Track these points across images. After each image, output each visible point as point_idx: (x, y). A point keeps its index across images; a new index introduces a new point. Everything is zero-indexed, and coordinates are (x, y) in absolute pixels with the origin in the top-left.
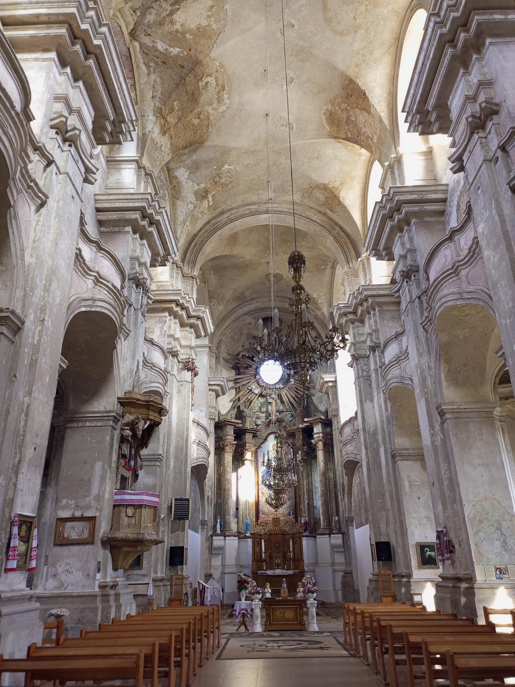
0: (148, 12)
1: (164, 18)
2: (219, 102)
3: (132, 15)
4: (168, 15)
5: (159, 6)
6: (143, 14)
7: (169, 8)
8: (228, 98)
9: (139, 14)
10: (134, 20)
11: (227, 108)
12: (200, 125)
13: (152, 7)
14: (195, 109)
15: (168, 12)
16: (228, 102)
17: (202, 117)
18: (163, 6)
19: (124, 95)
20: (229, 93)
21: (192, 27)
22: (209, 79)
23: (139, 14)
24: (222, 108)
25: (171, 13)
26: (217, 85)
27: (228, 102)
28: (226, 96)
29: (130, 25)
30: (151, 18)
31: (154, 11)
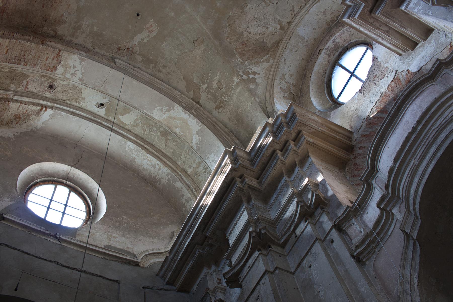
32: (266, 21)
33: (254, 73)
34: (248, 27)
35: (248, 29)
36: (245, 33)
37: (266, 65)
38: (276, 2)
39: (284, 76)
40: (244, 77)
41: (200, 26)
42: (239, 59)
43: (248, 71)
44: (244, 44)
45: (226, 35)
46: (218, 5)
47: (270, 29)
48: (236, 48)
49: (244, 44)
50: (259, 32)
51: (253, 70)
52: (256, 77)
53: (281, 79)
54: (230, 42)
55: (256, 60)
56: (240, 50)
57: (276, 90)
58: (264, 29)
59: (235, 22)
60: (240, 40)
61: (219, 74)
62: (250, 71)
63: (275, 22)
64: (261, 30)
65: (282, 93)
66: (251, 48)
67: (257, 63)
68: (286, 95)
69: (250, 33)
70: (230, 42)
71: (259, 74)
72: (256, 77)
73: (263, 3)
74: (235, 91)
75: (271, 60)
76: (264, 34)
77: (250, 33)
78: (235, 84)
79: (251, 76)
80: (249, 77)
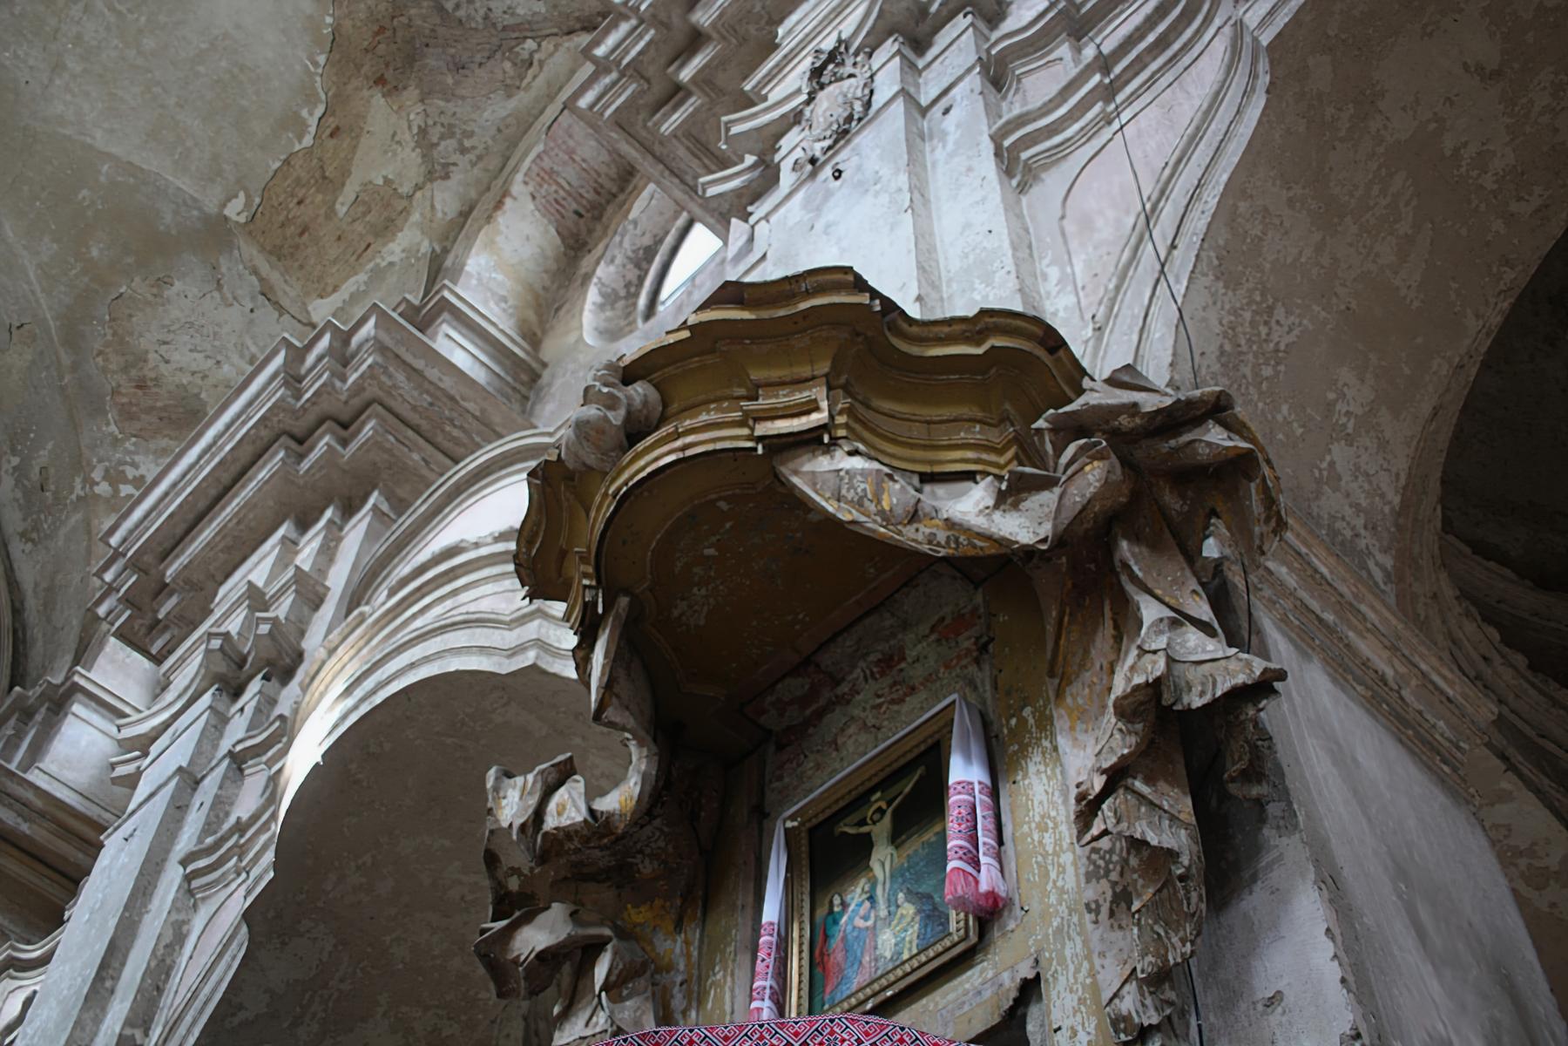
3: (541, 63)
10: (557, 47)
13: (486, 18)
19: (228, 427)
23: (530, 44)
32: (217, 343)
34: (165, 343)
35: (164, 347)
36: (152, 356)
38: (250, 306)
40: (103, 488)
41: (33, 292)
42: (113, 428)
43: (123, 472)
44: (141, 385)
45: (97, 346)
46: (95, 253)
47: (226, 367)
48: (115, 392)
49: (141, 385)
50: (194, 367)
54: (104, 370)
55: (164, 442)
56: (125, 400)
58: (210, 363)
59: (131, 316)
60: (133, 373)
61: (50, 446)
62: (131, 473)
63: (242, 356)
64: (200, 362)
66: (159, 404)
69: (167, 362)
70: (104, 370)
73: (216, 294)
74: (67, 517)
76: (205, 377)
77: (167, 362)
78: (74, 497)
80: (116, 491)
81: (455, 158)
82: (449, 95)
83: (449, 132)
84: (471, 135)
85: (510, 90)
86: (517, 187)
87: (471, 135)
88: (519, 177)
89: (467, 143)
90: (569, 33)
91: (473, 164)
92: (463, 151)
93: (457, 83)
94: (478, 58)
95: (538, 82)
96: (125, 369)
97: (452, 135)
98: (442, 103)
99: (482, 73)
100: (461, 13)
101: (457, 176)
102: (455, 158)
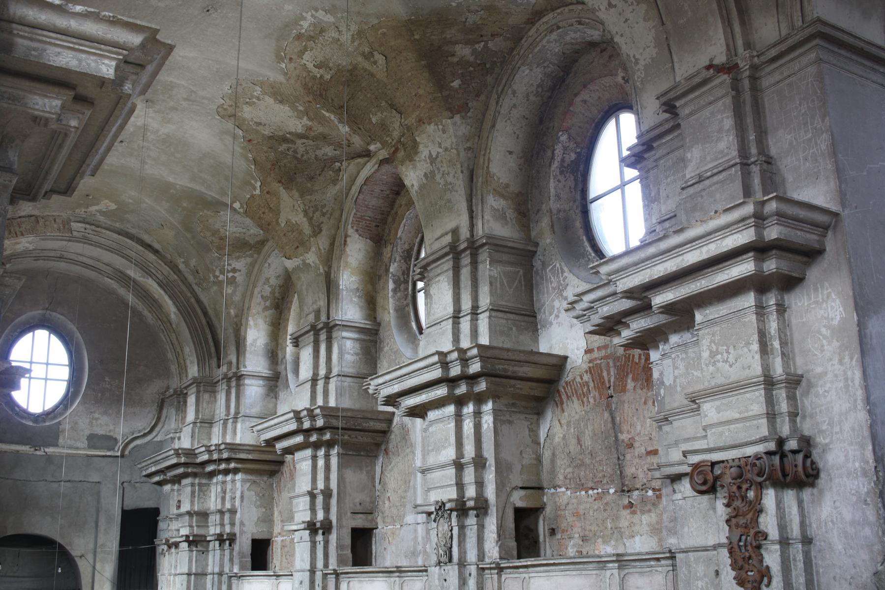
0: (325, 157)
1: (314, 139)
2: (322, 31)
4: (307, 138)
5: (307, 153)
6: (335, 159)
7: (299, 142)
8: (305, 19)
9: (337, 164)
10: (349, 164)
11: (317, 10)
12: (381, 45)
14: (366, 70)
15: (304, 141)
16: (308, 16)
17: (367, 50)
18: (304, 149)
20: (296, 22)
21: (287, 108)
22: (310, 66)
24: (326, 19)
25: (301, 136)
26: (306, 49)
27: (308, 16)
28: (305, 24)
29: (359, 163)
30: (328, 151)
31: (319, 153)
33: (234, 270)
37: (249, 260)
39: (268, 279)
49: (221, 239)
51: (233, 266)
52: (236, 275)
53: (264, 284)
55: (238, 254)
57: (257, 299)
65: (263, 303)
67: (238, 258)
68: (268, 303)
71: (240, 271)
72: (236, 275)
75: (255, 256)
79: (230, 275)
81: (322, 219)
82: (311, 192)
83: (316, 209)
84: (324, 206)
85: (335, 182)
86: (351, 231)
87: (324, 206)
88: (350, 226)
89: (324, 211)
90: (353, 158)
91: (329, 218)
92: (324, 215)
93: (313, 185)
94: (318, 173)
95: (345, 177)
96: (213, 235)
97: (317, 210)
98: (309, 197)
99: (321, 178)
100: (305, 157)
101: (325, 227)
102: (322, 219)
